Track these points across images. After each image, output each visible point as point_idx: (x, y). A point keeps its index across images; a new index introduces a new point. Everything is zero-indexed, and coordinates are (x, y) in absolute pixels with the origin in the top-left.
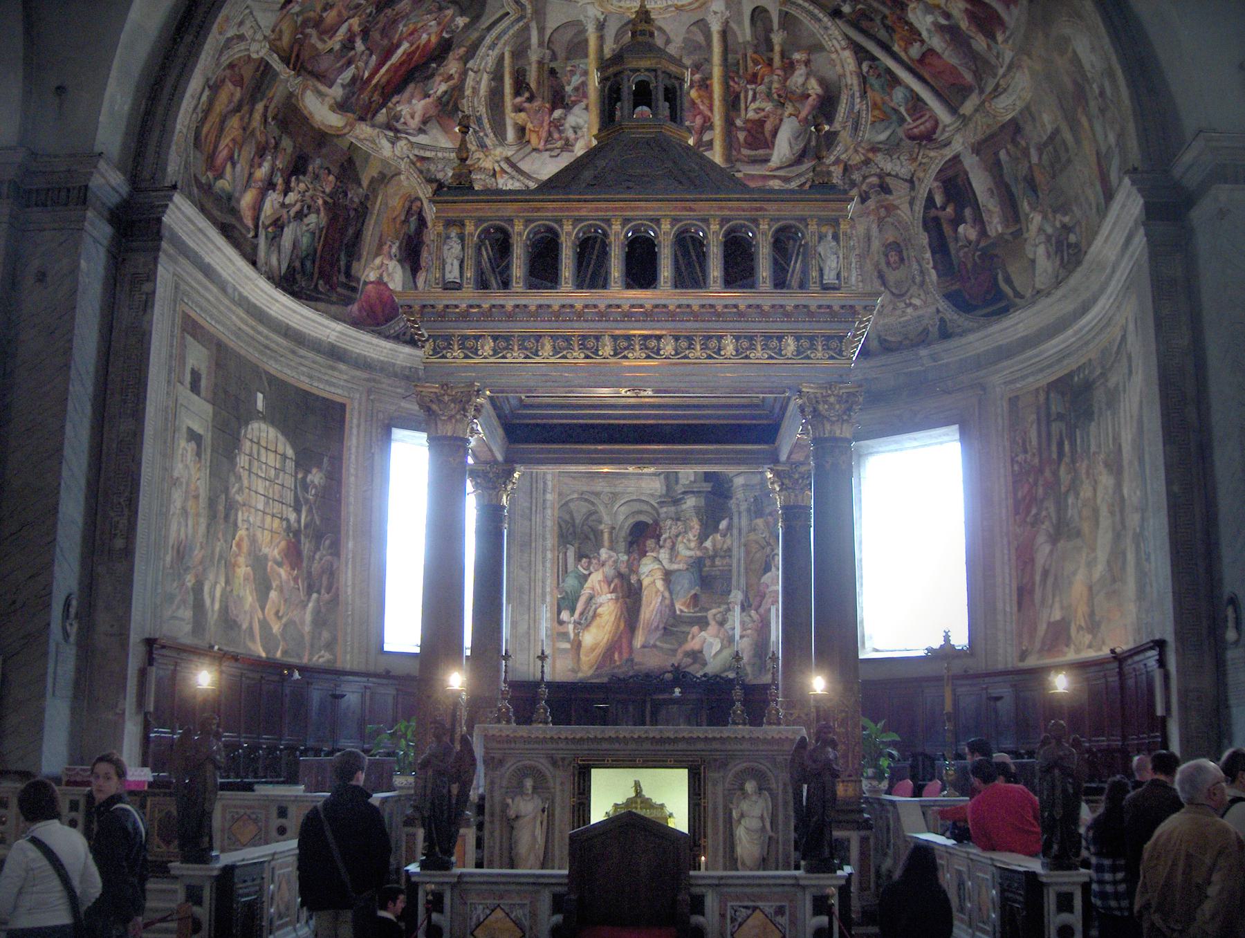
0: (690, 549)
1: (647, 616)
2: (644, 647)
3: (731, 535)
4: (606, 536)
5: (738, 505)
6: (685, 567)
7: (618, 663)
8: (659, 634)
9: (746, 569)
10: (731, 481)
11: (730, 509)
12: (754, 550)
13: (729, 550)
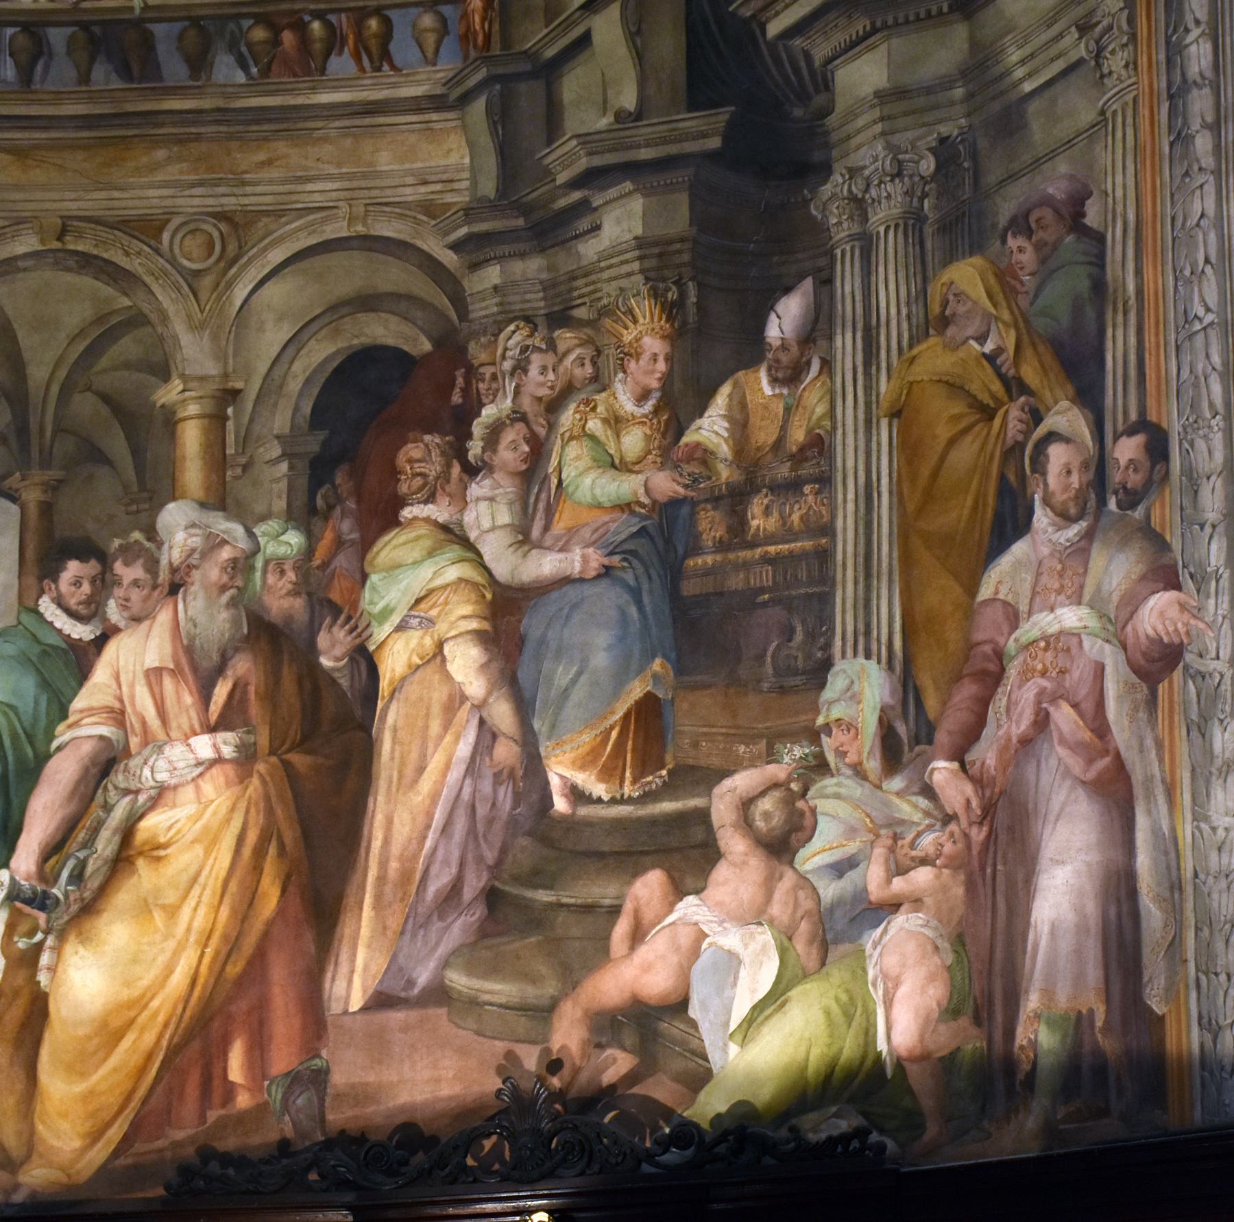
0: (619, 466)
1: (403, 830)
2: (380, 1001)
3: (827, 365)
4: (191, 437)
5: (859, 206)
6: (596, 559)
7: (243, 1100)
8: (458, 929)
9: (904, 535)
10: (825, 84)
11: (820, 229)
12: (943, 432)
13: (819, 445)
